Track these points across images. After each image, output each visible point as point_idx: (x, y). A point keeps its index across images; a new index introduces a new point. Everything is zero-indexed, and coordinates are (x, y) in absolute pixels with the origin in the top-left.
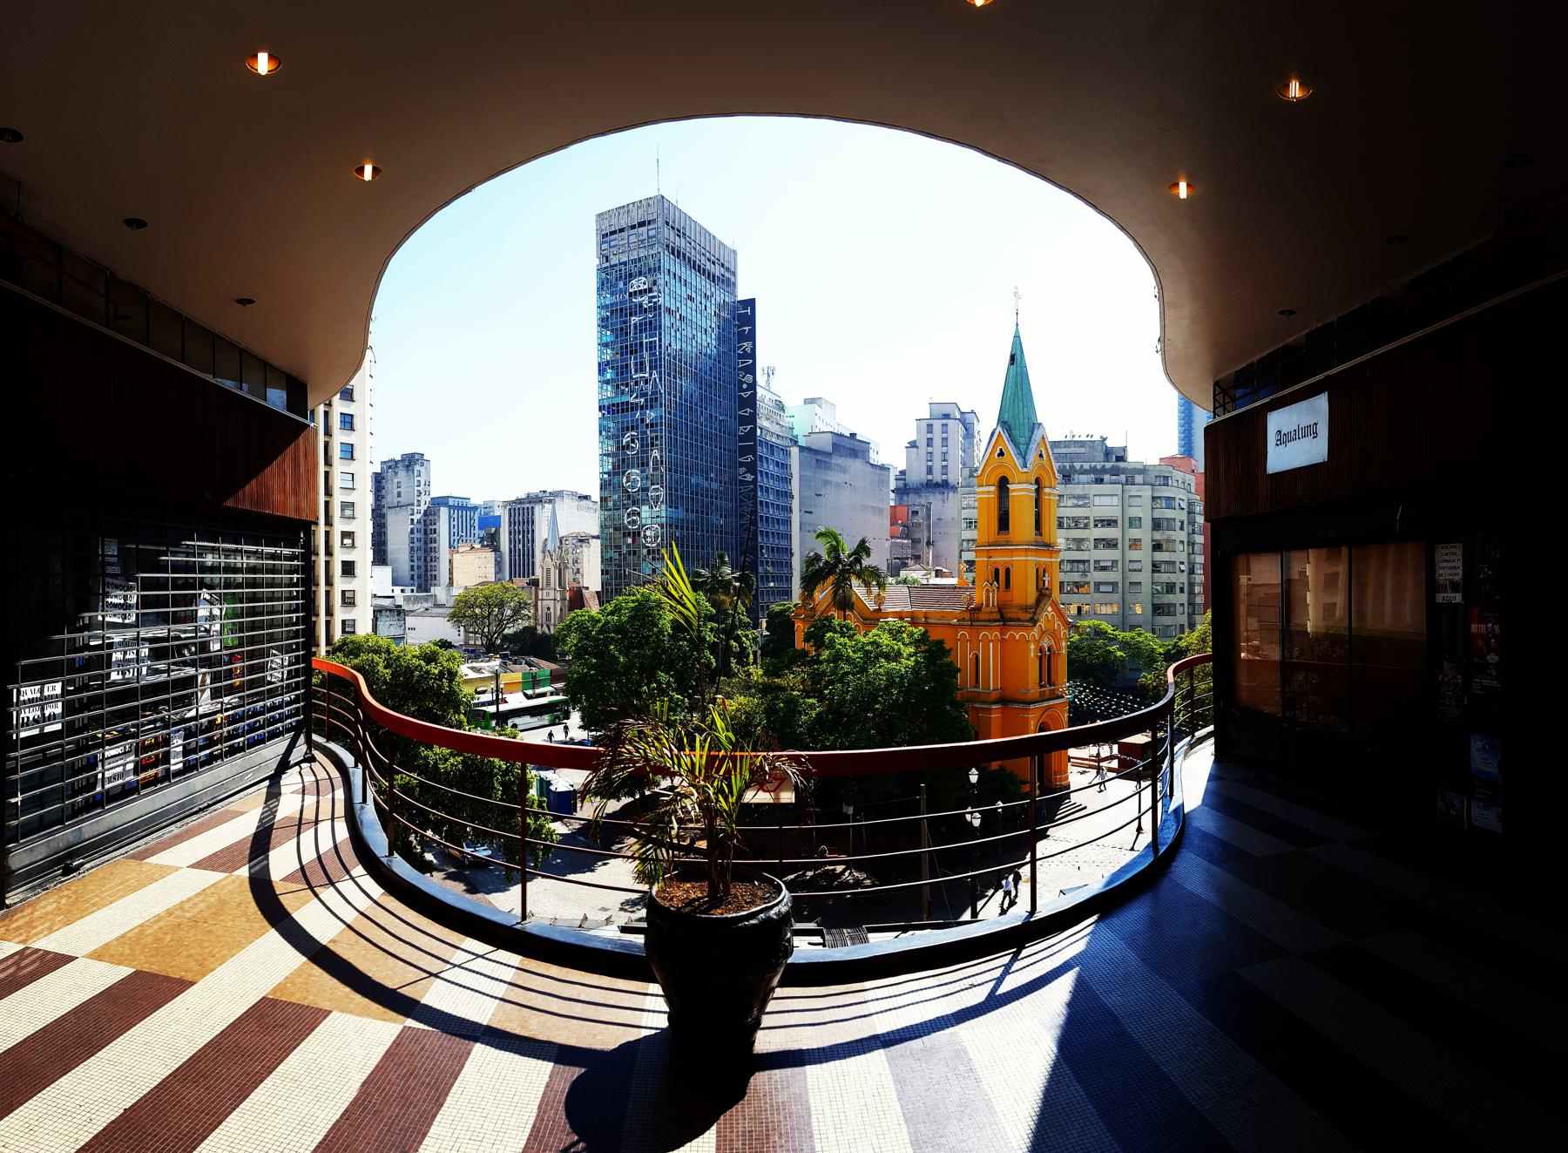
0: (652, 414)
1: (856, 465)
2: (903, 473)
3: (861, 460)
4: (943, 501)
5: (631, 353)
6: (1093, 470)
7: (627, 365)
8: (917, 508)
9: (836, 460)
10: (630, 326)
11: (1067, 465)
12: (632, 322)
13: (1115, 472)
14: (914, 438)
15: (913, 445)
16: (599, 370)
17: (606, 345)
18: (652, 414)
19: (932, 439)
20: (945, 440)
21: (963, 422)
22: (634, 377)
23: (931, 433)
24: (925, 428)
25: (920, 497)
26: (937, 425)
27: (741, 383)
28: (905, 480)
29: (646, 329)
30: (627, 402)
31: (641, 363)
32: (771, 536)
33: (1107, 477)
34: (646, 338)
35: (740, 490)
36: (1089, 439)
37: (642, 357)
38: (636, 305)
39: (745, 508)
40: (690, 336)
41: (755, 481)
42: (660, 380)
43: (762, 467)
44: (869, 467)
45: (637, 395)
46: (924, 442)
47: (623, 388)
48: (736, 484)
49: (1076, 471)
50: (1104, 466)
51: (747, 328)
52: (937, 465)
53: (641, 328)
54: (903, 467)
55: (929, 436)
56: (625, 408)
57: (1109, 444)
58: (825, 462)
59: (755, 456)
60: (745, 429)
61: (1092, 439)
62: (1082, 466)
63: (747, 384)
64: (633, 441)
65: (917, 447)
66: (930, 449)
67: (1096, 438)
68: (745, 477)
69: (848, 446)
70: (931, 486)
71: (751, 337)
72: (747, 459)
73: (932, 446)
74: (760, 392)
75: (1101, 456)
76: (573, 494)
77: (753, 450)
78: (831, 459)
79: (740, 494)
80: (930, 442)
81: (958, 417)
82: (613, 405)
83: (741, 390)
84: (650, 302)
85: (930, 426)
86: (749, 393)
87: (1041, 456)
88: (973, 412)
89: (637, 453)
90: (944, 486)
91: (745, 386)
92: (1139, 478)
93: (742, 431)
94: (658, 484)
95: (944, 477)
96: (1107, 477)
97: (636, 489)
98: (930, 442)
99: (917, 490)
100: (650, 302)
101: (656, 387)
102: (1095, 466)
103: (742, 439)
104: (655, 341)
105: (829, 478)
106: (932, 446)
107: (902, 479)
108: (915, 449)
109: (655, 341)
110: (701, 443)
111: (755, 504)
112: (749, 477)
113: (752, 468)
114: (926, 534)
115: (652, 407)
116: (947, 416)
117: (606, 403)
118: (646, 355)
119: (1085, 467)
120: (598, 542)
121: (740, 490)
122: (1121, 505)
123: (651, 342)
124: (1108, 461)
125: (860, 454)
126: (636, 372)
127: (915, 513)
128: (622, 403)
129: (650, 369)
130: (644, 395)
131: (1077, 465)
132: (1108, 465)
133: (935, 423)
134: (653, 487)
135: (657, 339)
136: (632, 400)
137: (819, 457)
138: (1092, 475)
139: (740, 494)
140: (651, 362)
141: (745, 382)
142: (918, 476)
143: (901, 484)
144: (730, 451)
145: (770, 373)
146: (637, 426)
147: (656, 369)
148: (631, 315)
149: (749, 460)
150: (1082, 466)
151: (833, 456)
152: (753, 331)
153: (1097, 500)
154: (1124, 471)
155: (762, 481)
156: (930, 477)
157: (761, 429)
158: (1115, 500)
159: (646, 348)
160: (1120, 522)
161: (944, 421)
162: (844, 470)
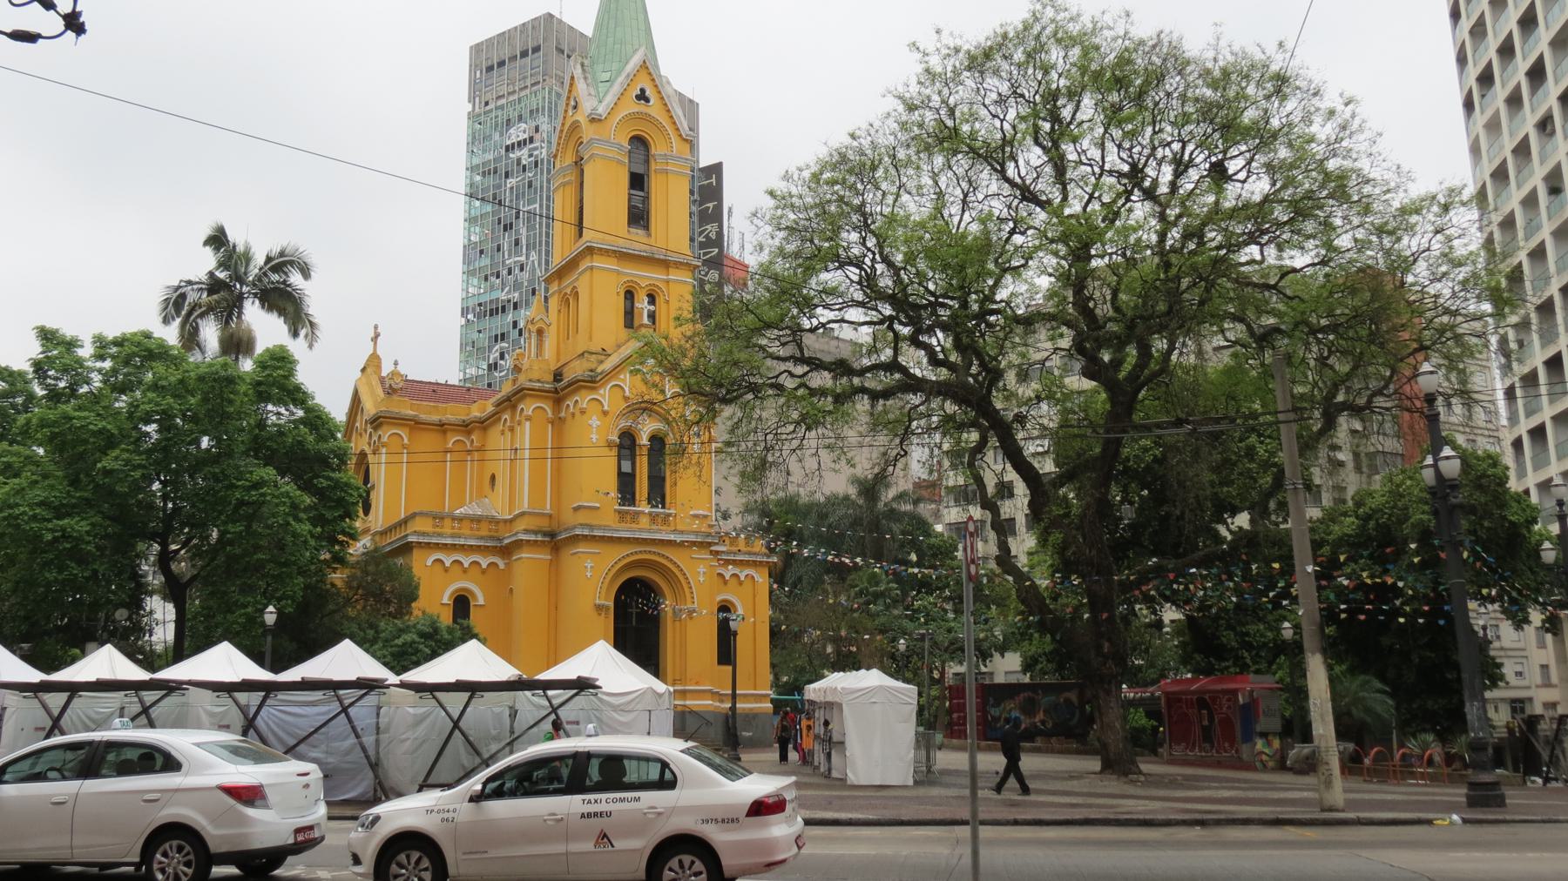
5: (505, 230)
30: (497, 299)
31: (517, 243)
37: (517, 232)
42: (540, 264)
47: (493, 279)
51: (711, 205)
56: (497, 310)
64: (502, 357)
82: (480, 305)
84: (531, 156)
89: (507, 375)
100: (531, 156)
117: (471, 304)
118: (524, 231)
126: (510, 255)
130: (517, 286)
135: (537, 206)
136: (503, 296)
148: (507, 176)
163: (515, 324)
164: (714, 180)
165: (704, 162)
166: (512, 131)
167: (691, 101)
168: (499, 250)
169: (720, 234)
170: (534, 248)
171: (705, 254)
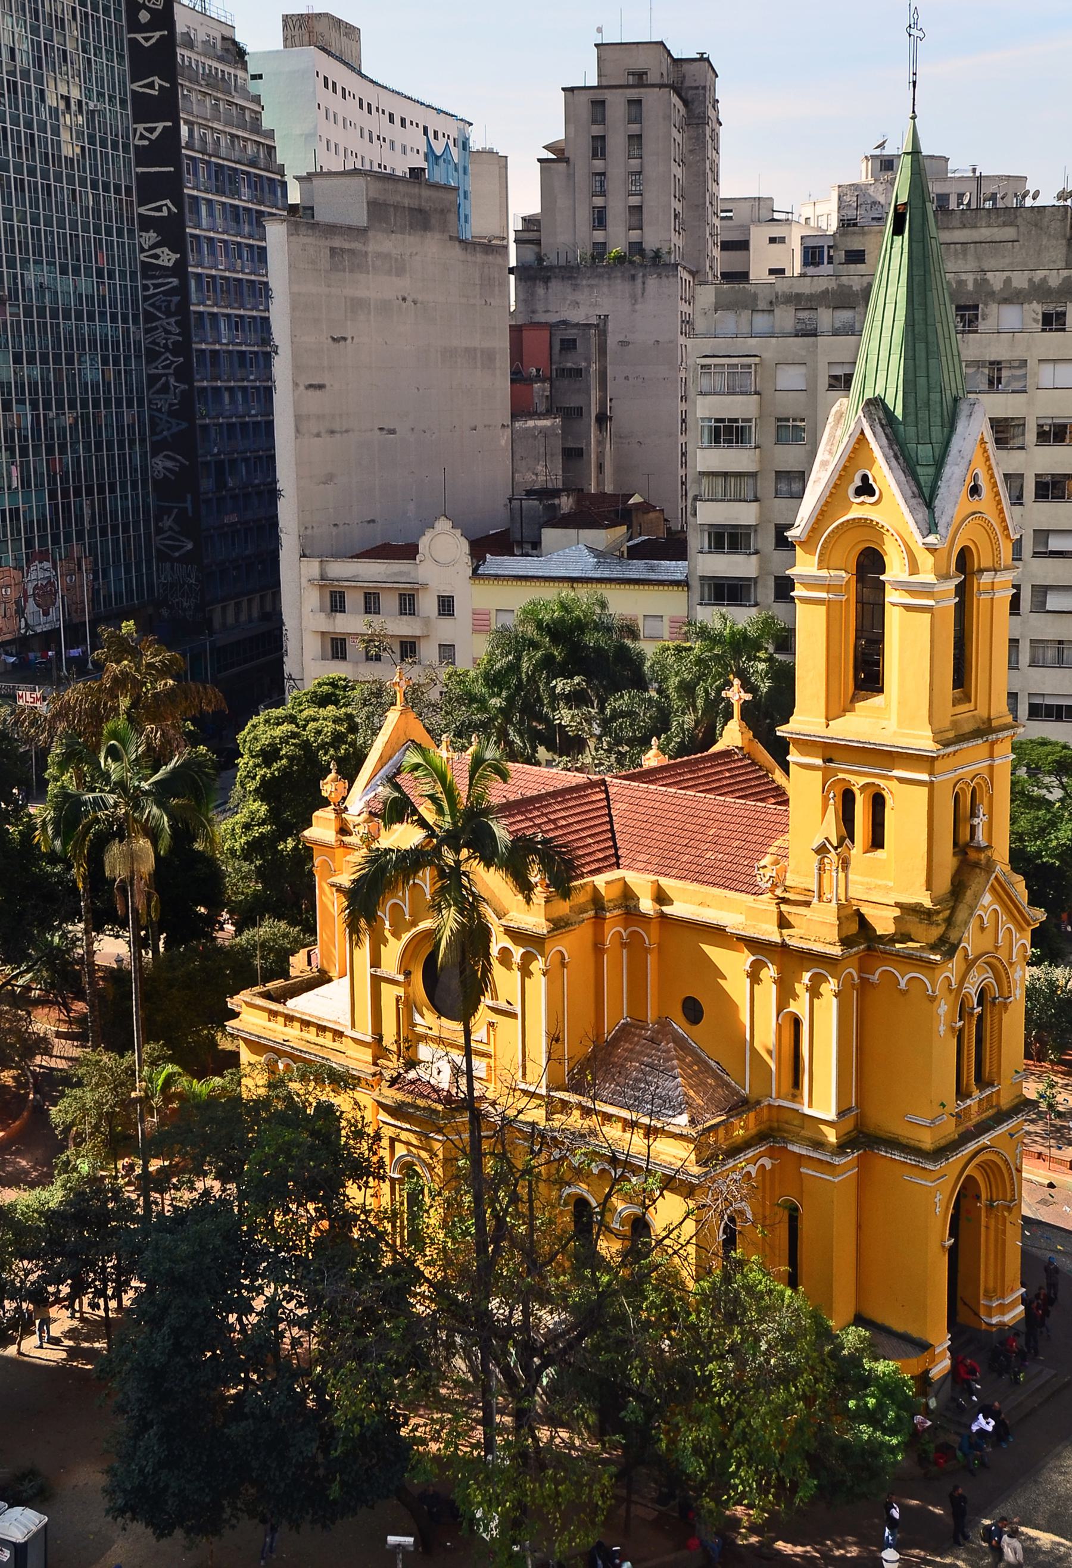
3: (438, 236)
6: (1039, 291)
8: (571, 333)
9: (382, 243)
11: (970, 279)
14: (557, 133)
19: (603, 138)
20: (636, 139)
21: (677, 89)
23: (603, 122)
24: (584, 111)
25: (575, 287)
28: (538, 242)
39: (160, 336)
41: (180, 269)
44: (456, 252)
48: (133, 274)
49: (992, 294)
54: (533, 207)
55: (597, 130)
58: (352, 252)
59: (178, 198)
60: (151, 130)
61: (1038, 203)
62: (1008, 281)
63: (149, 10)
65: (567, 161)
66: (599, 164)
69: (406, 202)
72: (159, 209)
77: (171, 187)
79: (146, 298)
80: (599, 147)
83: (135, 25)
85: (599, 105)
86: (157, 34)
88: (703, 59)
91: (144, 17)
93: (142, 137)
95: (634, 236)
98: (599, 147)
99: (569, 272)
102: (1044, 280)
103: (144, 156)
105: (362, 293)
108: (562, 166)
110: (45, 175)
111: (184, 325)
112: (167, 258)
114: (595, 395)
116: (640, 78)
125: (434, 221)
127: (569, 345)
131: (996, 280)
133: (608, 96)
137: (338, 242)
139: (146, 298)
144: (117, 191)
149: (165, 213)
150: (1008, 281)
151: (370, 234)
153: (1046, 375)
156: (599, 236)
161: (633, 94)
162: (398, 267)
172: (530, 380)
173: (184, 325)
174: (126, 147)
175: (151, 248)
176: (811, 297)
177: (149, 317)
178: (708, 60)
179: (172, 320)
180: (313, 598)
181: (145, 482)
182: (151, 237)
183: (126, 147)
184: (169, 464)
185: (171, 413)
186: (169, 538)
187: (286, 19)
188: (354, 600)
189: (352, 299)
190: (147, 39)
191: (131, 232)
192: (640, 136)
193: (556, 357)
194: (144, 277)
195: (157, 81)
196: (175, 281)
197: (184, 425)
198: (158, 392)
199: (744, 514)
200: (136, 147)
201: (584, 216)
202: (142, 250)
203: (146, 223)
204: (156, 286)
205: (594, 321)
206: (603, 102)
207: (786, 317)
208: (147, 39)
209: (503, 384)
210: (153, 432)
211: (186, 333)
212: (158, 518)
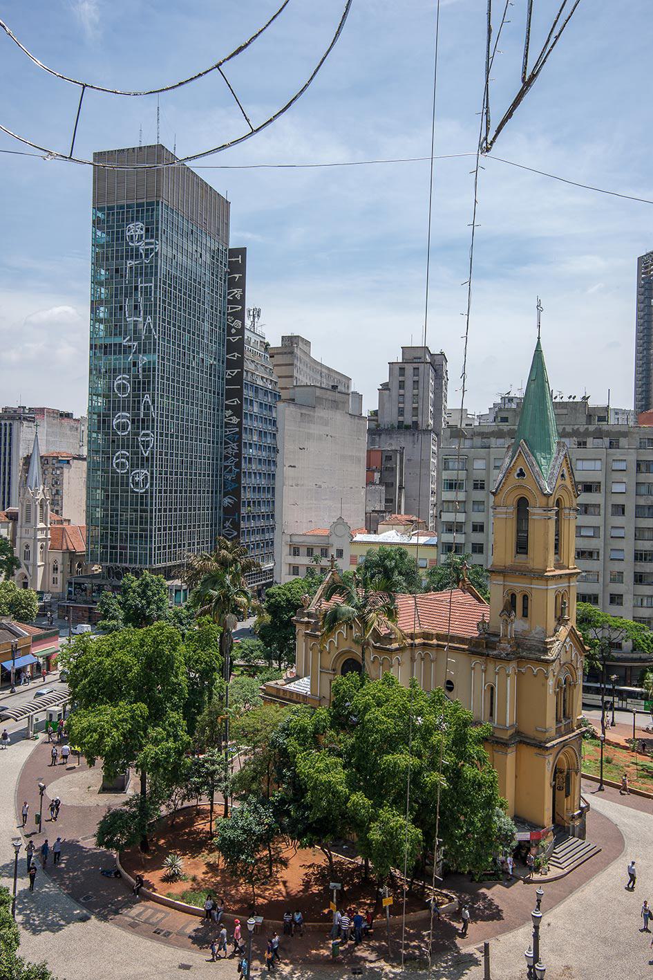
0: (145, 358)
1: (338, 417)
2: (375, 413)
3: (341, 412)
4: (414, 441)
6: (575, 433)
7: (121, 307)
10: (126, 268)
12: (128, 265)
13: (599, 434)
15: (385, 387)
16: (92, 308)
17: (100, 284)
18: (145, 358)
20: (416, 382)
22: (128, 319)
23: (403, 375)
24: (397, 372)
25: (391, 438)
26: (409, 369)
27: (230, 328)
28: (377, 421)
29: (141, 274)
31: (136, 307)
32: (253, 475)
33: (590, 441)
34: (141, 283)
35: (226, 432)
36: (571, 400)
37: (136, 301)
38: (132, 249)
39: (230, 450)
40: (170, 255)
41: (240, 425)
42: (155, 326)
43: (246, 408)
45: (131, 338)
46: (396, 385)
48: (222, 427)
50: (587, 429)
51: (237, 276)
52: (408, 407)
53: (138, 272)
55: (401, 379)
57: (591, 403)
60: (232, 373)
62: (564, 429)
63: (235, 328)
65: (389, 389)
66: (402, 392)
67: (578, 399)
68: (231, 420)
70: (402, 427)
71: (241, 284)
72: (233, 402)
73: (403, 389)
74: (247, 334)
75: (583, 419)
76: (54, 411)
77: (239, 394)
78: (314, 412)
80: (402, 385)
81: (429, 360)
83: (230, 334)
85: (402, 369)
86: (238, 337)
87: (563, 475)
88: (442, 354)
90: (413, 429)
91: (233, 331)
92: (623, 442)
93: (229, 375)
94: (148, 429)
95: (415, 419)
96: (590, 441)
97: (127, 433)
98: (402, 385)
99: (390, 431)
101: (150, 332)
102: (578, 429)
103: (229, 382)
104: (151, 286)
105: (311, 431)
106: (403, 389)
107: (374, 420)
109: (151, 286)
111: (239, 447)
112: (235, 420)
113: (238, 411)
115: (145, 352)
118: (141, 300)
119: (567, 430)
120: (84, 465)
121: (226, 432)
122: (604, 470)
123: (146, 287)
124: (590, 424)
127: (389, 458)
128: (115, 345)
129: (145, 313)
132: (592, 428)
133: (406, 366)
134: (143, 432)
136: (124, 342)
138: (575, 438)
140: (145, 306)
141: (234, 327)
142: (390, 418)
143: (373, 424)
145: (257, 313)
146: (129, 369)
147: (150, 314)
148: (127, 259)
149: (236, 403)
150: (564, 429)
152: (243, 279)
154: (608, 434)
155: (247, 423)
156: (401, 419)
157: (247, 372)
158: (598, 465)
159: (141, 292)
160: (602, 487)
161: (416, 365)
163: (135, 364)
164: (240, 259)
165: (232, 245)
166: (131, 226)
167: (227, 202)
168: (121, 309)
169: (243, 296)
170: (150, 314)
171: (232, 308)
172: (374, 471)
173: (239, 447)
174: (223, 379)
175: (229, 417)
176: (487, 433)
177: (226, 443)
178: (444, 355)
179: (235, 444)
180: (286, 550)
181: (220, 507)
182: (230, 412)
183: (223, 379)
184: (230, 501)
185: (232, 481)
186: (228, 530)
187: (283, 337)
188: (303, 550)
189: (308, 433)
190: (234, 339)
191: (222, 410)
192: (418, 381)
193: (383, 463)
194: (225, 428)
195: (236, 354)
196: (237, 429)
197: (237, 485)
198: (227, 472)
199: (461, 517)
200: (226, 379)
201: (395, 410)
202: (226, 417)
203: (228, 407)
204: (230, 431)
205: (399, 449)
206: (404, 368)
207: (478, 441)
208: (234, 339)
209: (363, 470)
210: (224, 488)
211: (240, 450)
212: (224, 522)
